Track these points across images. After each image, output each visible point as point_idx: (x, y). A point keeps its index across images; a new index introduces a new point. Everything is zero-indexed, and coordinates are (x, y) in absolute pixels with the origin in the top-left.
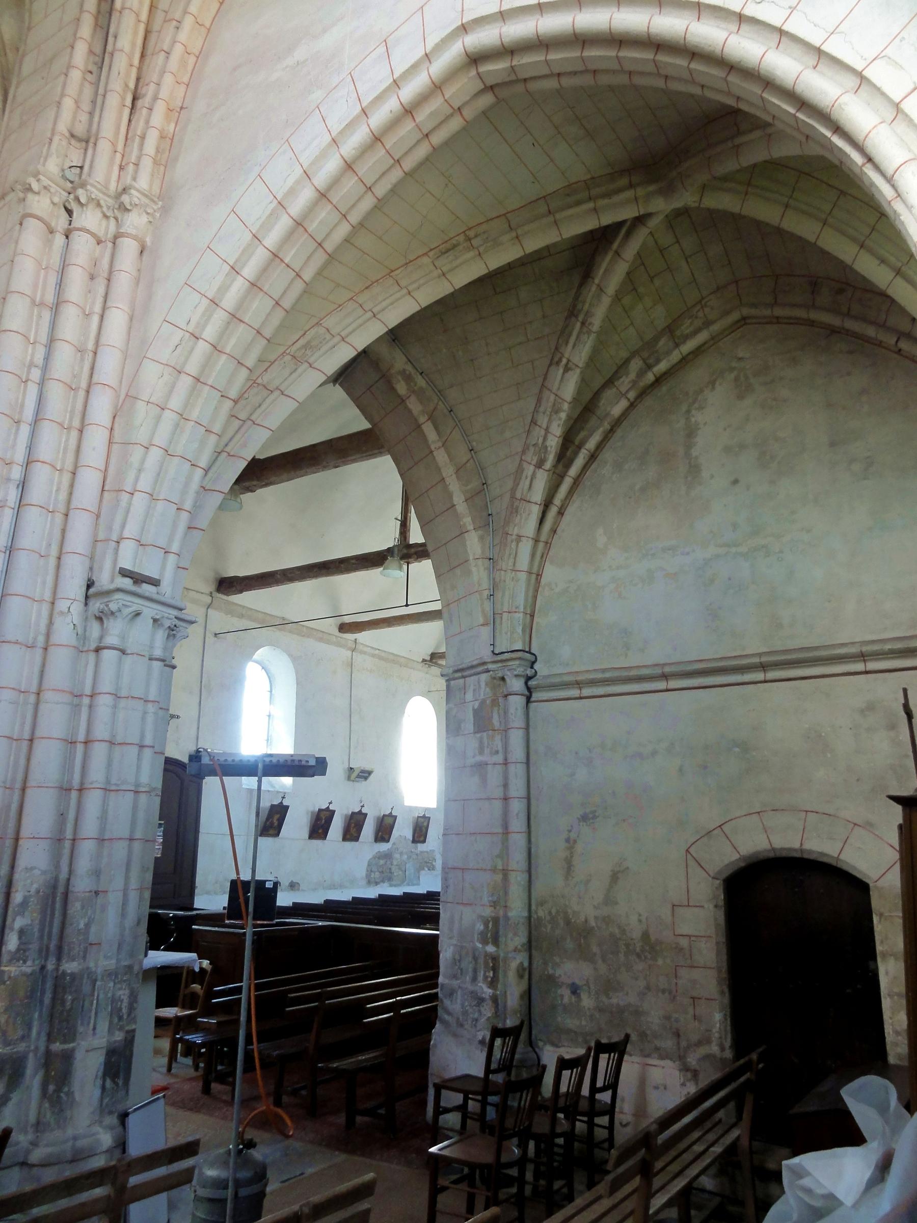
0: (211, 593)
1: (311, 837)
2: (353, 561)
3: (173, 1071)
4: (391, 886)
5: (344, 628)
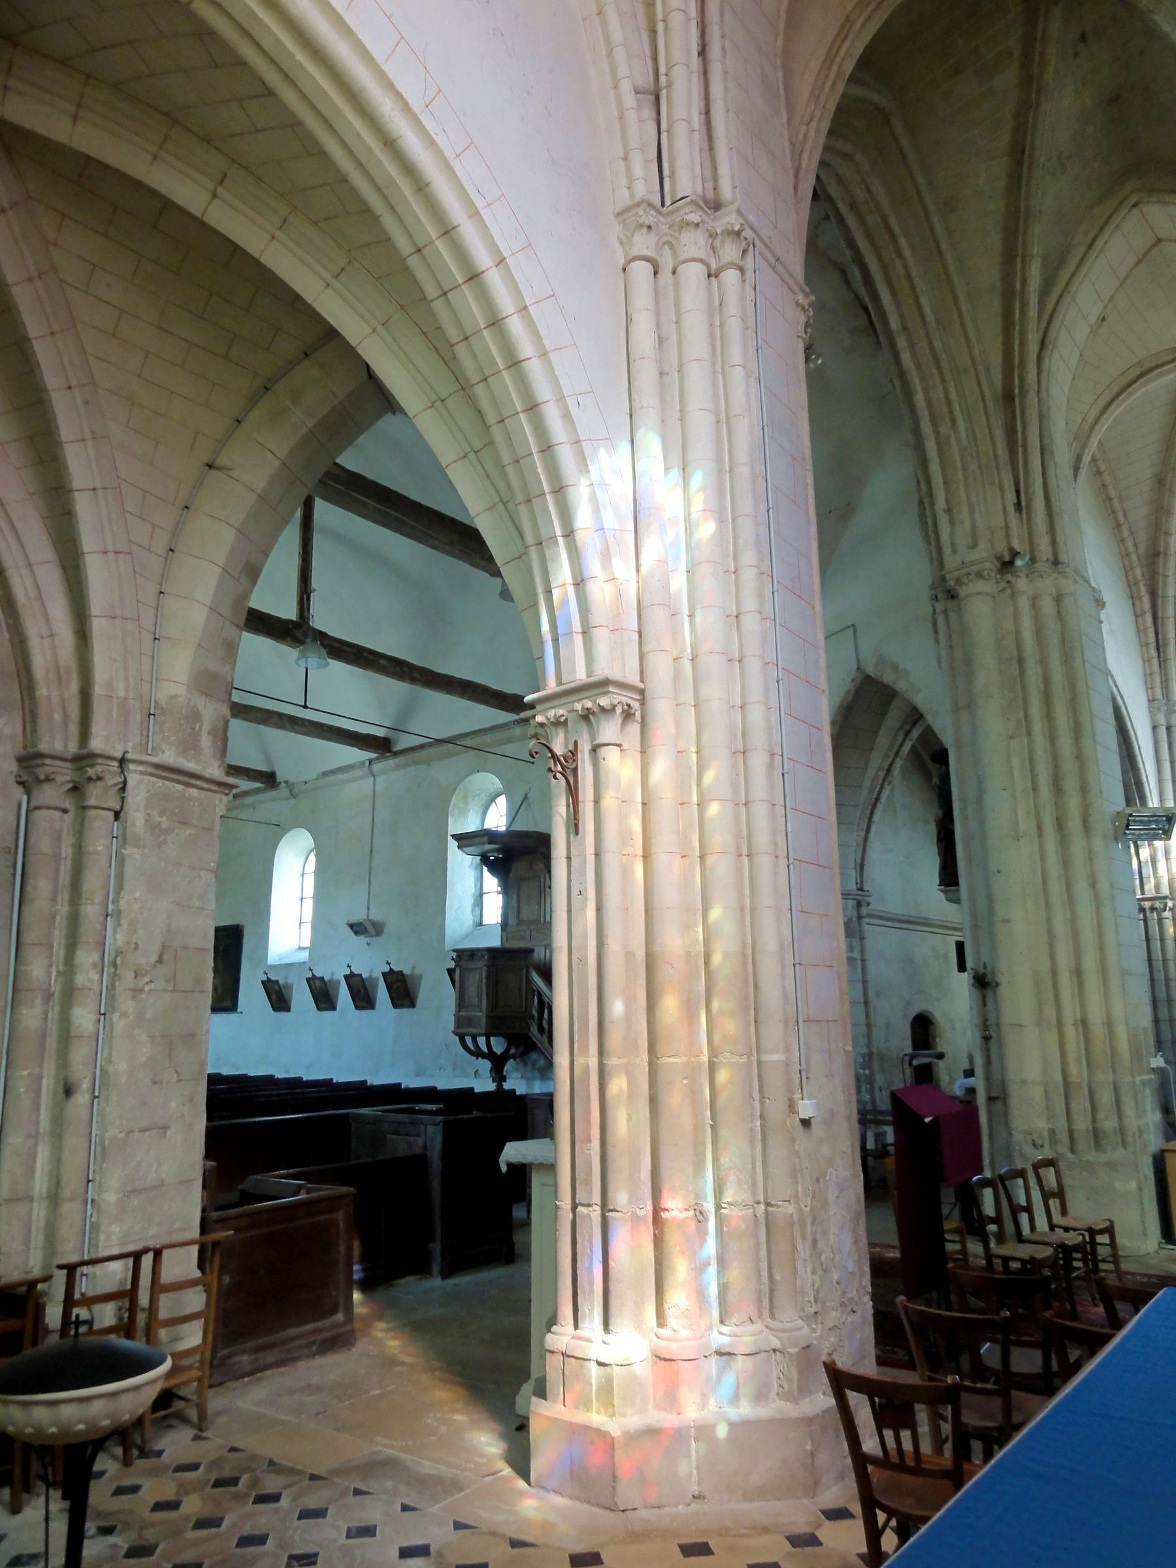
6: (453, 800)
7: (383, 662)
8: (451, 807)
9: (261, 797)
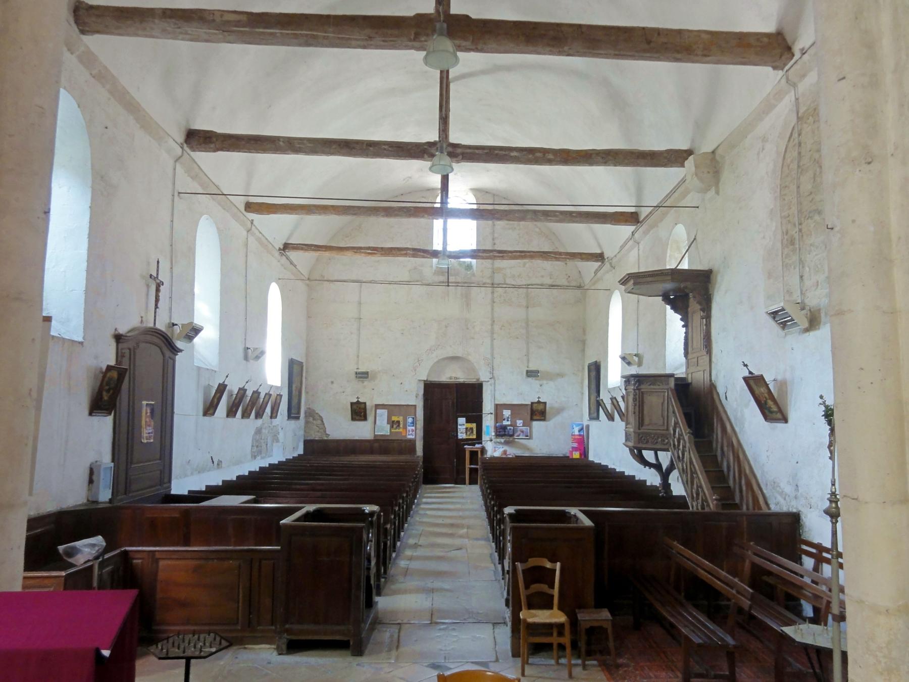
1: (228, 416)
2: (386, 147)
3: (526, 673)
4: (262, 458)
5: (249, 207)
6: (669, 251)
7: (514, 154)
8: (668, 259)
9: (602, 271)
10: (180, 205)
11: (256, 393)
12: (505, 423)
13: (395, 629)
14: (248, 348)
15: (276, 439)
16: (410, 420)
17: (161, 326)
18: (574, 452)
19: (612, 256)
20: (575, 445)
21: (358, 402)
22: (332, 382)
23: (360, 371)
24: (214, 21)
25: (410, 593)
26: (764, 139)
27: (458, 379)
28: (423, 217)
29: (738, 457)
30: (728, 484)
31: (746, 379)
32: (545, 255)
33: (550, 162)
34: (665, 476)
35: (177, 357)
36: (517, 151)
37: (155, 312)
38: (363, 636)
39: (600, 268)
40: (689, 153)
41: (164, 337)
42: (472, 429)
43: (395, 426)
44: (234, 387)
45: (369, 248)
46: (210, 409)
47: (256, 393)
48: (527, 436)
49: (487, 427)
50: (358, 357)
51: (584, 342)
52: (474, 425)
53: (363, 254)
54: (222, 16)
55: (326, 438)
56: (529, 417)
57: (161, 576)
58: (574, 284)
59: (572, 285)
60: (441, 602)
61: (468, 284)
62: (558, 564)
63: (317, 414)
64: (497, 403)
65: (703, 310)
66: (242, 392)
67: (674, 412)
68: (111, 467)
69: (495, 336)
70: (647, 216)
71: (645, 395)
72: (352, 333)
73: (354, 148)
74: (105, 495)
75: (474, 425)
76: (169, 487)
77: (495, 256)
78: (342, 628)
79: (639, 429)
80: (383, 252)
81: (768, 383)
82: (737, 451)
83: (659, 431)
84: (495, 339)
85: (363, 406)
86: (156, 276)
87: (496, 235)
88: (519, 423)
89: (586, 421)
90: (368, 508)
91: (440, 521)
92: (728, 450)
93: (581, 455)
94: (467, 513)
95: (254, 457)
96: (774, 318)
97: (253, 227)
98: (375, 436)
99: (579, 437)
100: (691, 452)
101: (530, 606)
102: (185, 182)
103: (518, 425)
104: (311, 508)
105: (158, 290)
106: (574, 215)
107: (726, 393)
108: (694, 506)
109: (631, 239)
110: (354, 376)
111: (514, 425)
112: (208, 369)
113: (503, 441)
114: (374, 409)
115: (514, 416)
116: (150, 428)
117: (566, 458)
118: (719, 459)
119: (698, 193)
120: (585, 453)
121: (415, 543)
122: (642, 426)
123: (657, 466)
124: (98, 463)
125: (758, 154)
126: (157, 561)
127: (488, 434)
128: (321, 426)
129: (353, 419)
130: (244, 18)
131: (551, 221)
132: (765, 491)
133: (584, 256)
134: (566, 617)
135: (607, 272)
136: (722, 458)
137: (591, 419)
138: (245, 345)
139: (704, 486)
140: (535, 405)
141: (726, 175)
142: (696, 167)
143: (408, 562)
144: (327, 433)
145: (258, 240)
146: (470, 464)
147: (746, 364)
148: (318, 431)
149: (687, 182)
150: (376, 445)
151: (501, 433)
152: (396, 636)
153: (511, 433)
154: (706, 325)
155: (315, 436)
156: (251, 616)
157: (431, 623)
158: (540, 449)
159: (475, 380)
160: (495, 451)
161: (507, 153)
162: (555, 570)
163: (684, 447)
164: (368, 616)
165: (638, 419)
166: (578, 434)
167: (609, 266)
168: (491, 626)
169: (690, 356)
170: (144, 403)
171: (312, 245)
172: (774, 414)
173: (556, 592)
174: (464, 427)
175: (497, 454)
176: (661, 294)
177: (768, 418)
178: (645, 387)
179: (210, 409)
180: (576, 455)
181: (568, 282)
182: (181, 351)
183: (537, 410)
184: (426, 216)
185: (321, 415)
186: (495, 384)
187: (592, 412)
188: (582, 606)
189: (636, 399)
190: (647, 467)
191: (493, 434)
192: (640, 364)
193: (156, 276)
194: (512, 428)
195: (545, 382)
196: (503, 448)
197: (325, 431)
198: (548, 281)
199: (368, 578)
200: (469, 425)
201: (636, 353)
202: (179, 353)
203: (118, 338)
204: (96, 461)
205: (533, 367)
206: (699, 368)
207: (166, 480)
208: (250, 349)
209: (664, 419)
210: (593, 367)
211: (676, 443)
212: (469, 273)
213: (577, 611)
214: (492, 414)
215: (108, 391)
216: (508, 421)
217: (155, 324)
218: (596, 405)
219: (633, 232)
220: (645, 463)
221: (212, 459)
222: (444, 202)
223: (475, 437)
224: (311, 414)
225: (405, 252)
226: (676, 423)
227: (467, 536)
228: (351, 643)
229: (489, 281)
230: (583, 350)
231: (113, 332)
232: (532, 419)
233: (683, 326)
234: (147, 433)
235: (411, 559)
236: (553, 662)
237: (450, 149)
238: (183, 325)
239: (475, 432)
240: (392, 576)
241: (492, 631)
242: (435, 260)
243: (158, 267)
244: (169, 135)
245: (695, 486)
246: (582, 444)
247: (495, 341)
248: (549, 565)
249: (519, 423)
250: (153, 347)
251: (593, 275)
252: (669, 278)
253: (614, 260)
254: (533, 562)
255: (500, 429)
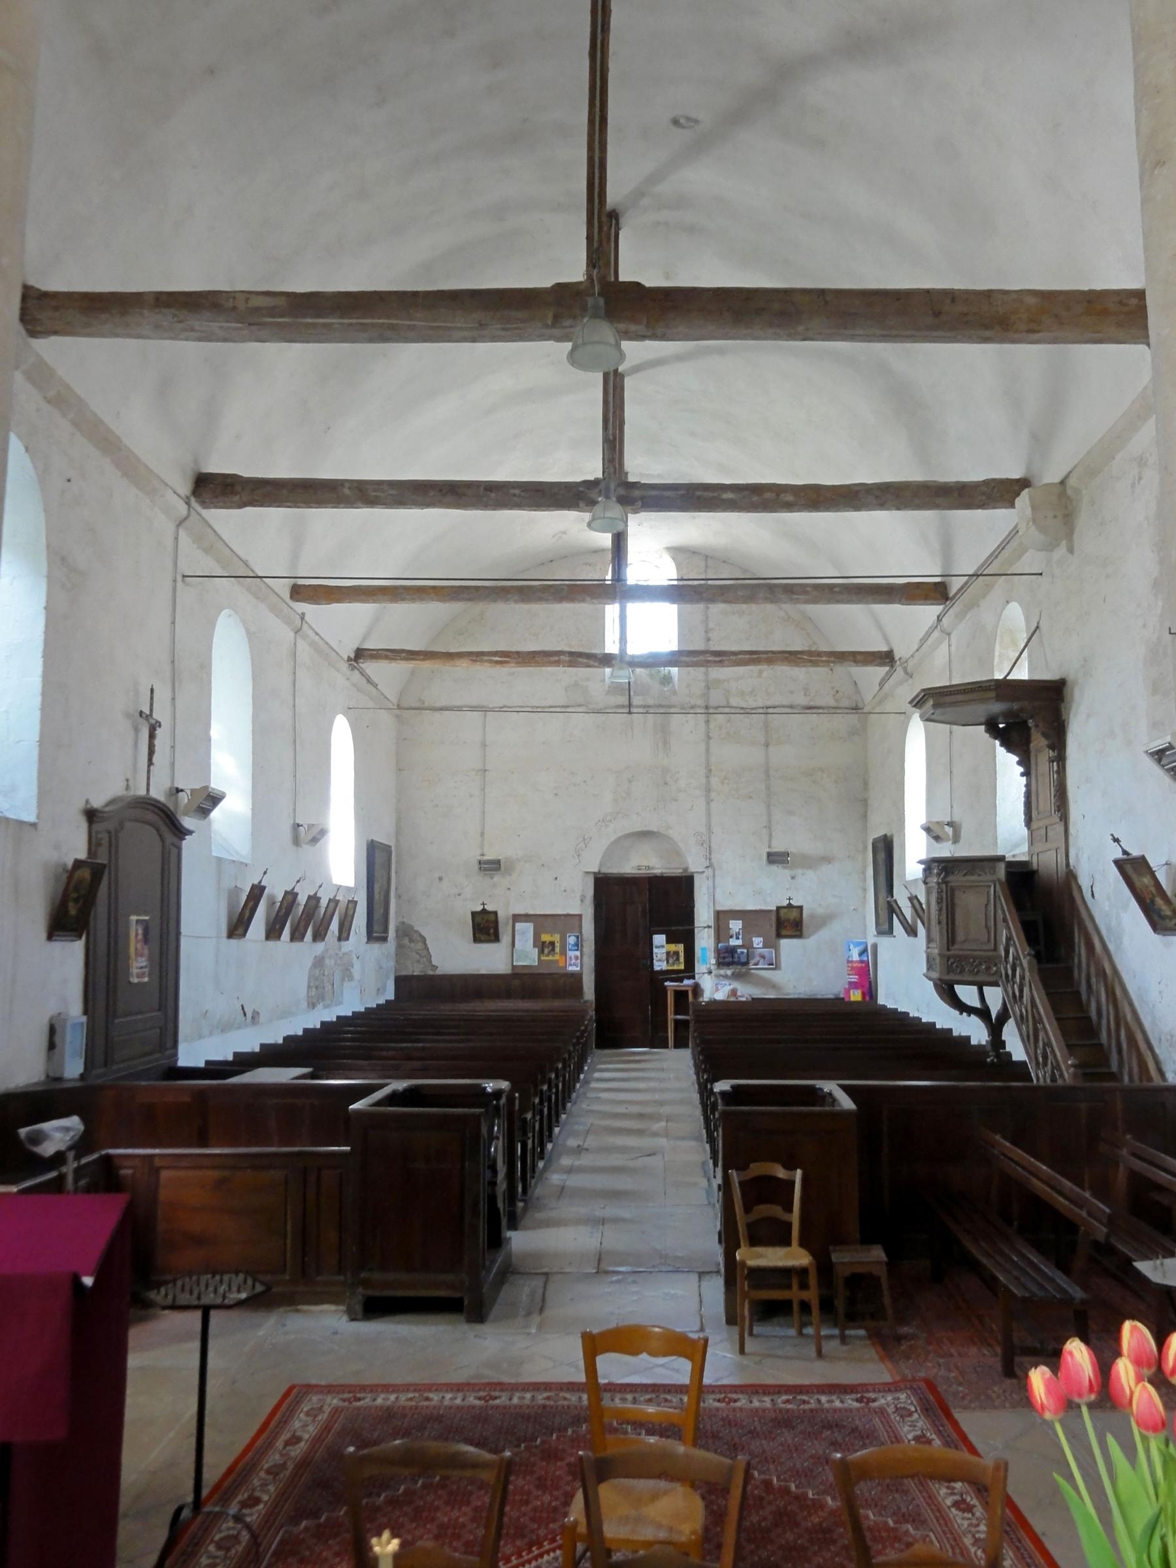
0: (187, 498)
1: (268, 938)
2: (517, 492)
3: (747, 1349)
4: (326, 1007)
5: (299, 592)
7: (729, 495)
8: (996, 661)
9: (891, 681)
10: (187, 595)
11: (314, 899)
12: (733, 942)
13: (538, 1283)
14: (299, 825)
15: (347, 974)
16: (572, 940)
17: (158, 793)
18: (852, 991)
19: (908, 657)
20: (854, 978)
21: (484, 911)
22: (440, 879)
23: (485, 858)
24: (234, 308)
25: (566, 1225)
26: (1141, 462)
27: (653, 868)
28: (583, 601)
29: (1114, 994)
30: (1099, 1039)
31: (1117, 863)
32: (791, 657)
33: (789, 507)
34: (995, 1029)
35: (184, 842)
36: (732, 492)
37: (149, 771)
38: (484, 1291)
39: (888, 676)
40: (1024, 483)
41: (162, 810)
42: (677, 953)
43: (546, 951)
44: (276, 889)
45: (496, 653)
46: (238, 926)
47: (314, 899)
48: (772, 964)
49: (703, 949)
50: (482, 834)
51: (865, 802)
52: (680, 948)
53: (486, 664)
54: (247, 299)
55: (431, 973)
56: (773, 931)
57: (163, 1195)
58: (846, 703)
59: (841, 705)
60: (614, 1240)
61: (664, 710)
62: (799, 1172)
63: (416, 931)
64: (719, 908)
65: (1052, 747)
66: (290, 897)
67: (1005, 920)
68: (82, 1024)
69: (713, 795)
70: (962, 588)
71: (958, 894)
72: (471, 796)
73: (464, 495)
74: (73, 1068)
75: (680, 948)
76: (175, 1055)
77: (709, 661)
78: (450, 1277)
79: (948, 949)
80: (520, 660)
81: (1154, 869)
82: (1112, 983)
83: (979, 953)
84: (712, 800)
85: (492, 917)
86: (148, 713)
87: (711, 625)
88: (758, 942)
89: (871, 937)
90: (490, 1086)
91: (621, 1109)
92: (1097, 981)
93: (864, 995)
94: (667, 1096)
95: (312, 1005)
96: (1159, 761)
97: (305, 627)
98: (514, 967)
99: (860, 965)
100: (1033, 987)
101: (754, 1241)
102: (194, 559)
103: (755, 946)
104: (399, 1085)
105: (152, 736)
106: (837, 589)
107: (1092, 887)
108: (1039, 1077)
109: (936, 627)
110: (476, 867)
111: (748, 945)
112: (234, 861)
113: (729, 972)
114: (511, 922)
115: (748, 931)
116: (144, 959)
117: (838, 1000)
118: (1084, 997)
119: (1041, 550)
120: (870, 991)
121: (579, 1146)
122: (952, 945)
123: (983, 1013)
124: (62, 1016)
125: (1133, 486)
126: (156, 1171)
127: (705, 961)
128: (425, 953)
129: (476, 940)
130: (282, 301)
131: (797, 601)
132: (1157, 1051)
133: (859, 657)
134: (811, 1258)
135: (901, 683)
136: (1089, 997)
137: (880, 933)
138: (295, 820)
139: (1054, 1043)
140: (783, 912)
141: (1083, 520)
142: (1033, 508)
143: (564, 1177)
144: (434, 963)
145: (312, 644)
146: (676, 1013)
147: (1116, 837)
148: (418, 961)
149: (1020, 533)
150: (516, 982)
151: (726, 960)
152: (540, 1291)
153: (743, 959)
154: (1058, 772)
155: (416, 970)
156: (306, 1259)
157: (597, 1273)
158: (794, 987)
159: (681, 871)
160: (717, 990)
161: (716, 494)
162: (793, 1183)
163: (1022, 978)
164: (493, 1262)
165: (945, 931)
166: (858, 959)
167: (902, 673)
168: (695, 1277)
169: (1034, 825)
170: (134, 918)
171: (403, 651)
172: (1168, 920)
173: (795, 1217)
174: (664, 950)
175: (720, 996)
176: (983, 720)
177: (1158, 927)
178: (956, 879)
179: (238, 926)
180: (856, 996)
181: (836, 700)
182: (190, 832)
183: (788, 920)
184: (588, 599)
185: (423, 934)
186: (714, 876)
187: (881, 921)
188: (841, 1241)
189: (942, 900)
190: (965, 1014)
191: (713, 961)
192: (956, 839)
193: (148, 713)
194: (745, 951)
195: (799, 871)
196: (730, 985)
197: (431, 962)
198: (802, 700)
199: (492, 1199)
200: (673, 947)
201: (949, 820)
202: (187, 837)
203: (91, 815)
204: (60, 1014)
205: (778, 847)
206: (1048, 845)
207: (169, 1045)
208: (301, 826)
209: (989, 932)
210: (881, 845)
211: (1010, 972)
212: (666, 689)
213: (831, 1248)
214: (709, 927)
215: (76, 900)
216: (738, 938)
217: (148, 790)
218: (888, 912)
219: (938, 617)
220: (962, 1007)
221: (243, 1008)
222: (618, 576)
223: (682, 967)
224: (407, 933)
225: (557, 659)
226: (1009, 939)
227: (666, 1134)
228: (466, 1303)
229: (700, 702)
230: (865, 816)
231: (81, 805)
232: (779, 936)
233: (1022, 775)
234: (137, 968)
235: (570, 1170)
236: (792, 1332)
237: (621, 491)
238: (192, 790)
239: (682, 959)
240: (538, 1198)
241: (697, 1285)
242: (608, 670)
243: (152, 698)
244: (166, 485)
245: (1041, 1044)
246: (866, 977)
247: (713, 805)
248: (781, 1173)
249: (758, 942)
250: (147, 827)
251: (878, 688)
252: (993, 694)
253: (911, 664)
254: (757, 1169)
255: (724, 953)
